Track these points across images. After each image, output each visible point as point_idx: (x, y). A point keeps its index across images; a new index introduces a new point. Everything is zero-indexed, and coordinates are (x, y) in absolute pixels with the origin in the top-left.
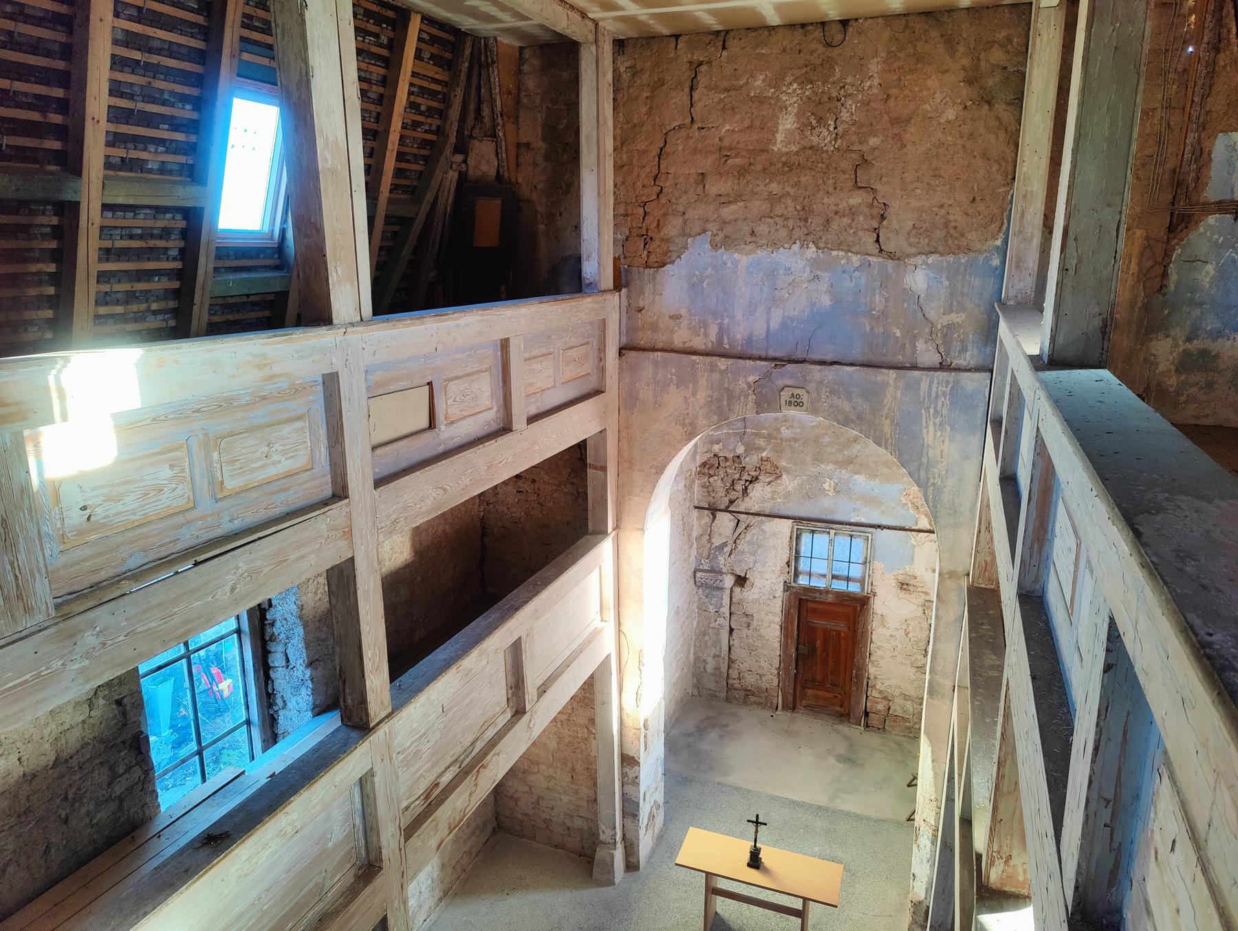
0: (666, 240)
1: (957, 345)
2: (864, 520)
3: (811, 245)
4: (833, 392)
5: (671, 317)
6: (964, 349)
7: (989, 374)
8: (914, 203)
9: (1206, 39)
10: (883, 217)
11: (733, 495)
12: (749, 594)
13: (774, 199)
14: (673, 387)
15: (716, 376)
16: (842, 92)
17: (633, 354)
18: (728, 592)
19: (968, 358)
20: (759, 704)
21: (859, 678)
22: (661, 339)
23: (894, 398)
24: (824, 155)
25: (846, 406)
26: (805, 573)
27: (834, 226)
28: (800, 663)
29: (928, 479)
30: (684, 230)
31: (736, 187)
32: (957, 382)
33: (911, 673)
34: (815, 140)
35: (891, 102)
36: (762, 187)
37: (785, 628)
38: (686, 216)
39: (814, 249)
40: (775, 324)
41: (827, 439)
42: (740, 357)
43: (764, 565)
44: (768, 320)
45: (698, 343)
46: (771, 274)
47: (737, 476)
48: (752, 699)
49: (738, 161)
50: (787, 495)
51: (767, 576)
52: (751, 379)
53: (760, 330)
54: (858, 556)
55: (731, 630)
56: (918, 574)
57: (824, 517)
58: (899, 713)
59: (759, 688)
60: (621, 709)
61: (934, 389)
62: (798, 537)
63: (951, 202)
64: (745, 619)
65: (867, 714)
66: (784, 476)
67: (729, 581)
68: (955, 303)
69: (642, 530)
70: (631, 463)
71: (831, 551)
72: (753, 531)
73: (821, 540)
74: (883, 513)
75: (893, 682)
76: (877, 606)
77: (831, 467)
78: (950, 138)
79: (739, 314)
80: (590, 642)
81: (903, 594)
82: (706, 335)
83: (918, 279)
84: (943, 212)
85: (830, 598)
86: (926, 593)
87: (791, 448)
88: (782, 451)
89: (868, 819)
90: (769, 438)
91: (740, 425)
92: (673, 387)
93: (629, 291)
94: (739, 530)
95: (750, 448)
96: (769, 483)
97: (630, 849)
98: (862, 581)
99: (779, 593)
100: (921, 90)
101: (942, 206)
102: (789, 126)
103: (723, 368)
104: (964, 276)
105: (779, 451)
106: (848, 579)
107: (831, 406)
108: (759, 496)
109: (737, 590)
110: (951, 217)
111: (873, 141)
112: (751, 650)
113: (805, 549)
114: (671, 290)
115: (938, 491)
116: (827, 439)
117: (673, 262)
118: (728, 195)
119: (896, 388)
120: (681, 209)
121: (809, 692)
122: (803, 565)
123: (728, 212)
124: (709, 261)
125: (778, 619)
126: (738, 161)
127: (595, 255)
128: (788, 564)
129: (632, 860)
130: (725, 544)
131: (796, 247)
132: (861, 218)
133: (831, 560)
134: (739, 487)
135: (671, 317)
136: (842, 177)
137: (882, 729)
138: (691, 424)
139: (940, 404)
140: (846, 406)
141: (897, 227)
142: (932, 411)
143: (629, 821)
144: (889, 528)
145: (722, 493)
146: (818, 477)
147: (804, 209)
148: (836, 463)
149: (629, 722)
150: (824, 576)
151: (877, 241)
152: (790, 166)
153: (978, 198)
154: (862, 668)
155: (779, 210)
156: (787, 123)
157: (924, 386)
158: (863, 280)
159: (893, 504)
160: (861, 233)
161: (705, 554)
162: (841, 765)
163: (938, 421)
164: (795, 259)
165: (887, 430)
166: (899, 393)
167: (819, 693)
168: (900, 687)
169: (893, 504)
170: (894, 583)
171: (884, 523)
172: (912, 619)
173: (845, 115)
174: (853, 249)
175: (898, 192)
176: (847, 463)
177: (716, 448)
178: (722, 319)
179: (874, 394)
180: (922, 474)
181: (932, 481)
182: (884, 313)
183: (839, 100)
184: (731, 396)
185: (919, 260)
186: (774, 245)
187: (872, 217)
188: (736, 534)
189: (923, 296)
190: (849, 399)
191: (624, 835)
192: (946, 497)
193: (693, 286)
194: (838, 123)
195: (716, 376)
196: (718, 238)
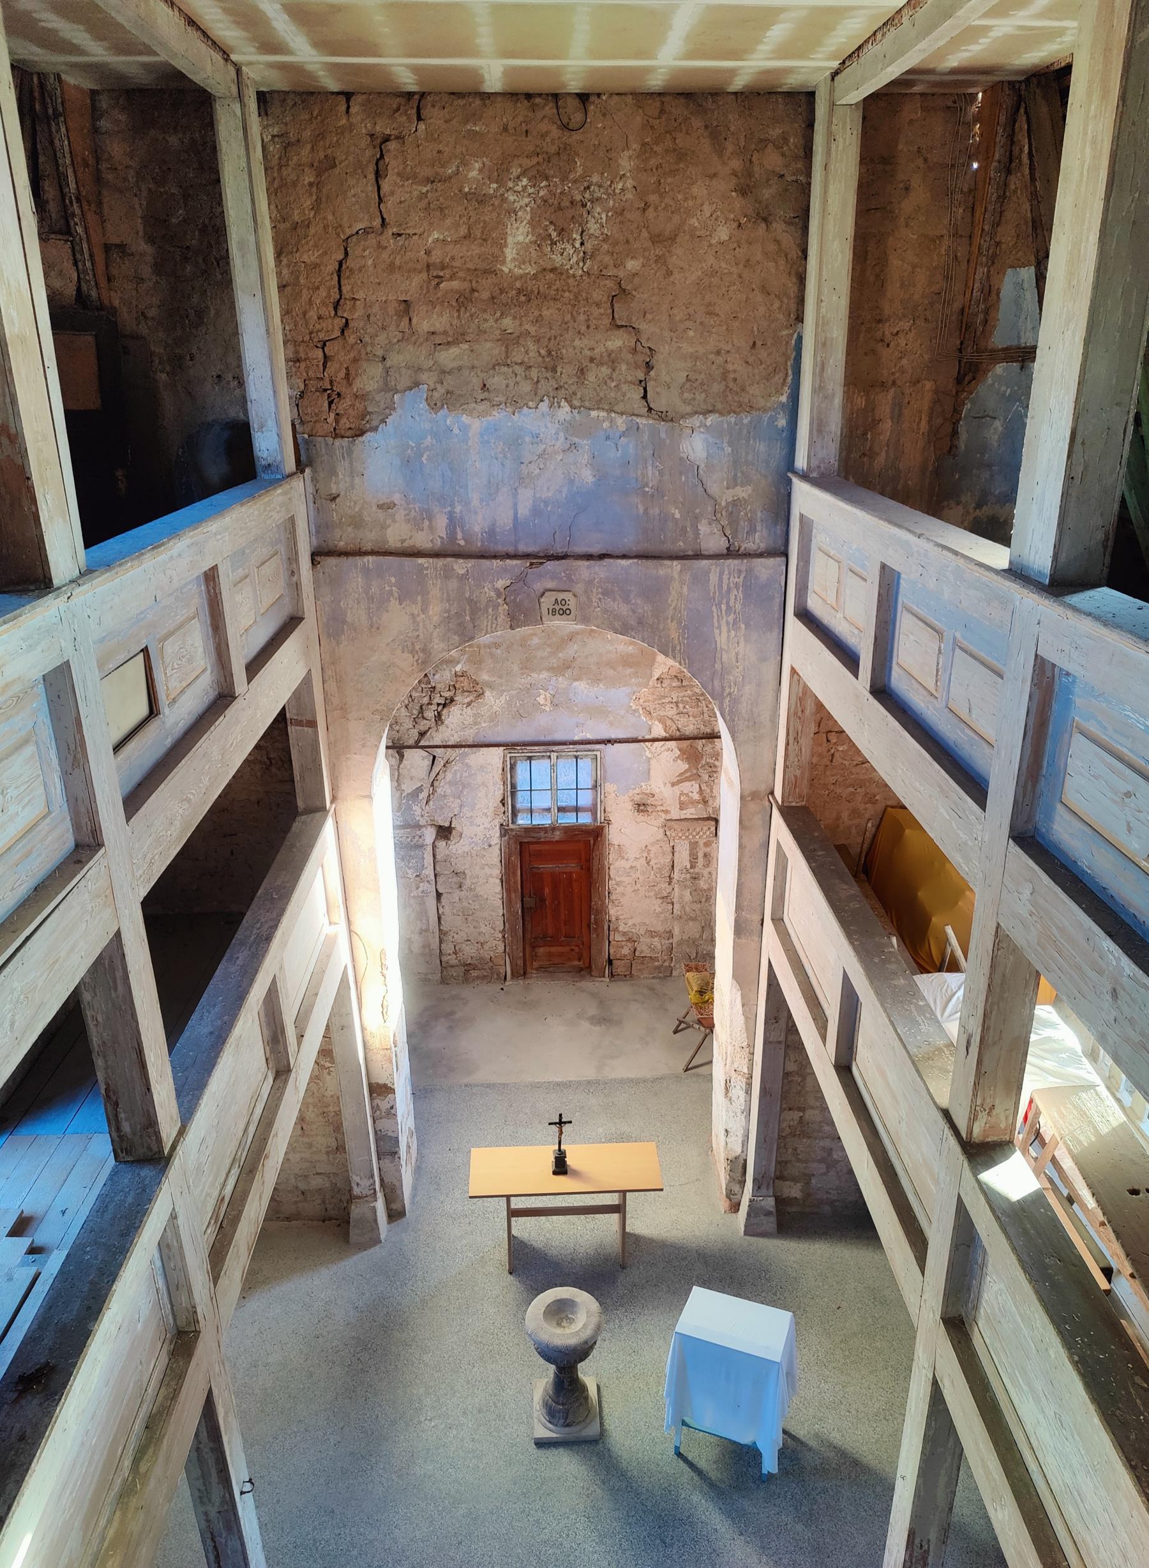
0: (361, 397)
1: (744, 525)
2: (589, 736)
3: (563, 403)
4: (606, 593)
5: (380, 507)
6: (752, 530)
7: (784, 559)
8: (687, 348)
9: (997, 156)
10: (649, 367)
11: (423, 725)
12: (456, 847)
13: (509, 341)
14: (394, 604)
15: (453, 584)
16: (587, 195)
17: (332, 561)
18: (430, 849)
19: (757, 541)
20: (484, 977)
21: (599, 923)
22: (369, 538)
23: (680, 595)
24: (571, 281)
25: (624, 610)
26: (524, 810)
27: (591, 377)
28: (527, 919)
29: (723, 688)
30: (386, 383)
31: (455, 322)
32: (750, 571)
33: (656, 905)
34: (558, 260)
35: (650, 213)
36: (491, 322)
37: (506, 881)
38: (388, 363)
39: (568, 409)
40: (524, 510)
42: (482, 556)
44: (515, 505)
45: (422, 540)
46: (515, 442)
47: (426, 700)
48: (474, 973)
49: (455, 284)
50: (494, 718)
51: (478, 821)
52: (501, 584)
53: (505, 519)
54: (586, 781)
55: (439, 895)
56: (656, 791)
57: (542, 738)
58: (647, 953)
59: (482, 959)
60: (363, 1029)
61: (725, 581)
63: (729, 347)
64: (455, 879)
65: (610, 962)
66: (487, 693)
67: (430, 835)
68: (739, 475)
69: (370, 797)
70: (344, 709)
71: (554, 780)
72: (455, 767)
73: (541, 767)
74: (611, 724)
75: (637, 920)
76: (614, 835)
77: (544, 675)
78: (724, 265)
79: (475, 499)
80: (329, 956)
81: (640, 817)
82: (431, 527)
83: (696, 445)
84: (719, 360)
85: (557, 836)
86: (667, 812)
87: (492, 655)
88: (481, 662)
89: (645, 1081)
92: (394, 604)
93: (314, 471)
94: (436, 769)
96: (469, 704)
97: (392, 1193)
98: (593, 810)
99: (496, 839)
100: (686, 199)
101: (718, 353)
102: (521, 238)
103: (461, 572)
104: (748, 440)
106: (577, 809)
107: (605, 611)
108: (458, 722)
109: (442, 844)
110: (730, 367)
111: (632, 265)
112: (466, 915)
114: (376, 469)
115: (735, 701)
116: (535, 641)
117: (375, 429)
118: (445, 333)
119: (682, 583)
120: (380, 353)
121: (541, 951)
122: (522, 801)
123: (448, 357)
124: (427, 426)
125: (497, 872)
126: (455, 284)
127: (271, 423)
128: (503, 802)
129: (394, 1206)
130: (420, 789)
131: (544, 406)
132: (624, 367)
133: (554, 789)
134: (430, 714)
135: (380, 507)
136: (596, 312)
137: (629, 976)
138: (424, 650)
139: (732, 598)
140: (624, 610)
141: (668, 379)
142: (724, 607)
143: (387, 1162)
144: (620, 741)
145: (408, 724)
146: (530, 689)
147: (549, 353)
149: (375, 1043)
150: (548, 810)
151: (645, 397)
152: (525, 296)
153: (759, 343)
154: (602, 911)
155: (517, 355)
156: (518, 235)
157: (714, 578)
158: (631, 449)
159: (622, 712)
160: (625, 387)
162: (598, 1028)
163: (731, 618)
164: (544, 422)
165: (674, 635)
166: (685, 589)
167: (553, 949)
169: (622, 712)
171: (613, 736)
172: (653, 844)
173: (593, 227)
174: (615, 408)
175: (666, 334)
176: (564, 667)
178: (452, 505)
179: (655, 592)
180: (716, 683)
181: (727, 690)
182: (659, 491)
183: (584, 206)
184: (475, 608)
185: (696, 420)
186: (515, 403)
187: (637, 367)
188: (433, 774)
189: (702, 466)
190: (627, 601)
191: (382, 1180)
192: (744, 708)
193: (407, 462)
194: (585, 238)
195: (453, 584)
196: (436, 395)
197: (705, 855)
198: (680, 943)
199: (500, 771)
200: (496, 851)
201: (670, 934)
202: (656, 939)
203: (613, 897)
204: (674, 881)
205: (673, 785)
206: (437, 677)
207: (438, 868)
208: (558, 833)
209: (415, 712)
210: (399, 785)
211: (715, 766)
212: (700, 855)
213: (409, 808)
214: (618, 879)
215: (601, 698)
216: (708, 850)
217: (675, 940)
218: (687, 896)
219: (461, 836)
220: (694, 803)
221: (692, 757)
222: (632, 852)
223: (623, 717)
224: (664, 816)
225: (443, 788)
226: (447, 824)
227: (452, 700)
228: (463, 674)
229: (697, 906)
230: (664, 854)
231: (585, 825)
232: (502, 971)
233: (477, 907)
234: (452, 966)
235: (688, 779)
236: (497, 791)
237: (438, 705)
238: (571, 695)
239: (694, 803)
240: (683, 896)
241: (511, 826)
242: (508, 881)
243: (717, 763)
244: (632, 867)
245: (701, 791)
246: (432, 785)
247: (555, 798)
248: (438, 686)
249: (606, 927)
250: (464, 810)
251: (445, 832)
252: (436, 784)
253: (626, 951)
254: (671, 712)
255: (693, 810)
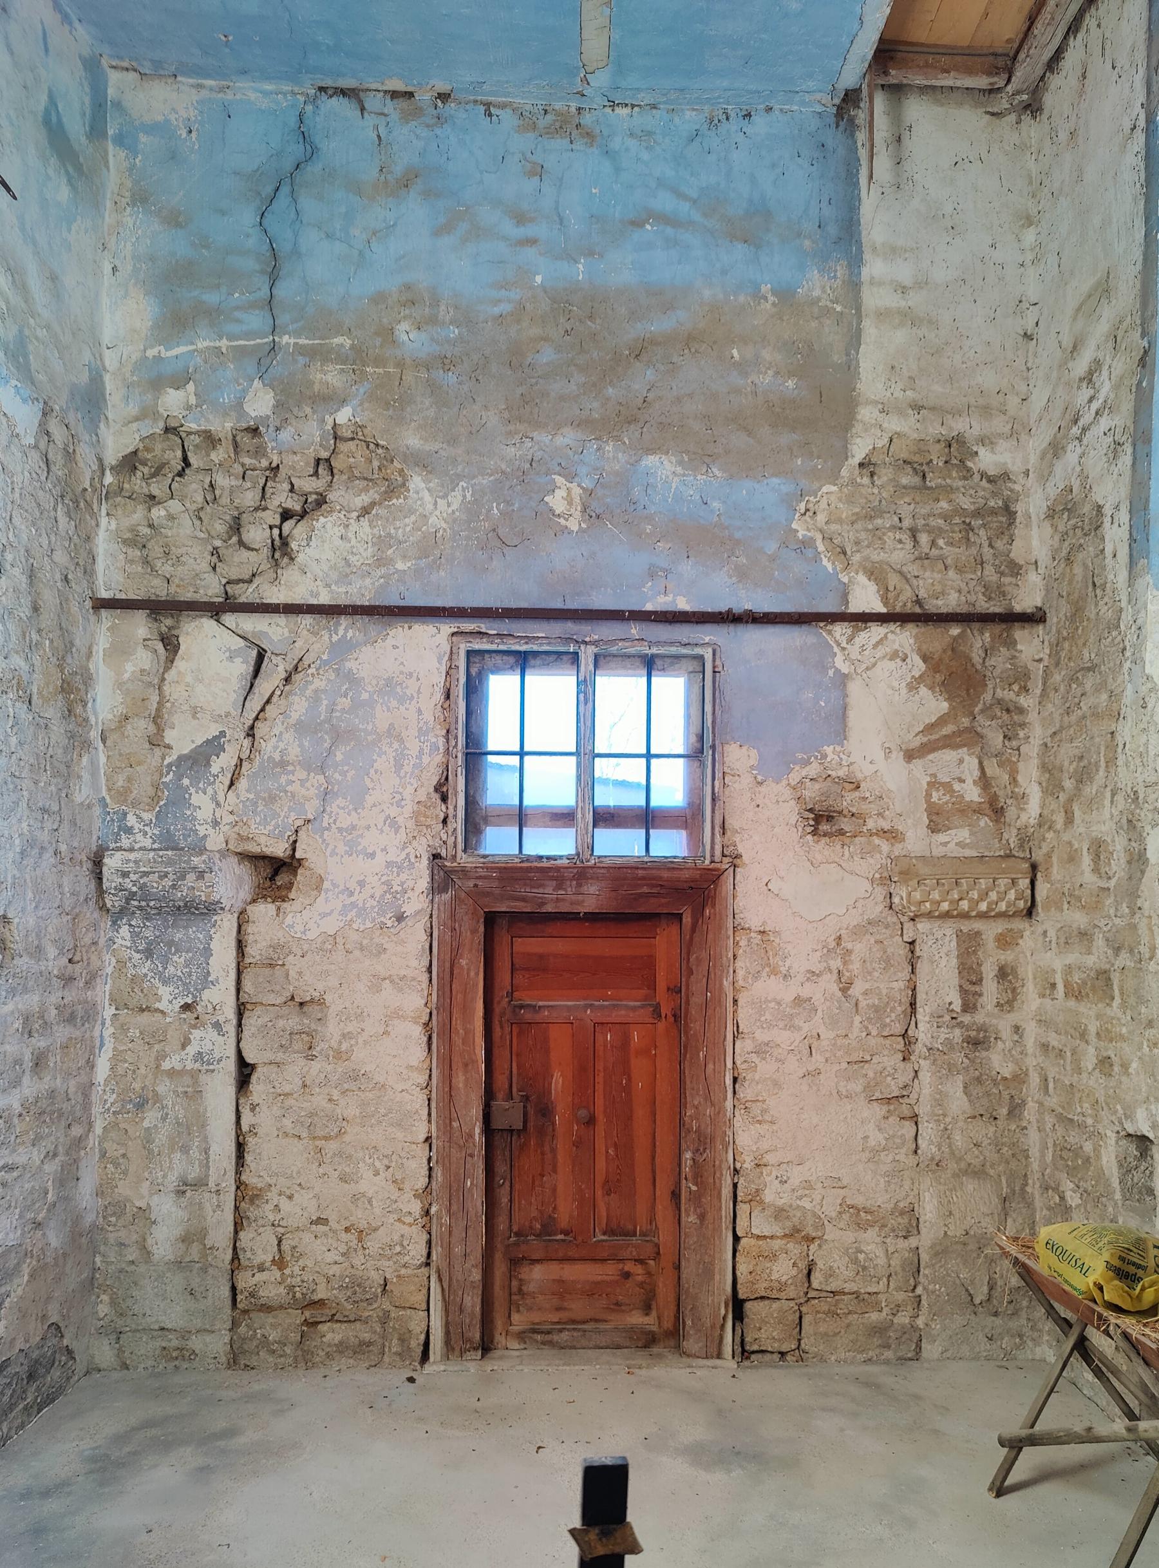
11: (240, 563)
12: (306, 918)
18: (227, 924)
20: (361, 1348)
33: (870, 1123)
37: (440, 1031)
41: (547, 356)
43: (358, 804)
47: (250, 498)
48: (332, 1334)
50: (429, 547)
51: (371, 840)
54: (672, 734)
55: (245, 1072)
56: (863, 770)
57: (558, 604)
58: (844, 1277)
59: (356, 1284)
62: (474, 690)
64: (293, 1022)
65: (738, 1307)
66: (416, 482)
67: (230, 884)
72: (317, 682)
74: (742, 574)
77: (568, 437)
81: (822, 849)
85: (591, 897)
86: (892, 835)
90: (357, 359)
91: (256, 320)
94: (265, 686)
95: (293, 398)
96: (365, 511)
98: (686, 819)
99: (417, 902)
105: (392, 401)
106: (648, 818)
108: (332, 555)
109: (263, 911)
113: (499, 732)
121: (537, 1275)
122: (499, 789)
130: (214, 746)
133: (585, 753)
134: (257, 534)
145: (196, 560)
146: (529, 477)
148: (583, 423)
150: (563, 818)
159: (771, 547)
161: (143, 788)
162: (718, 1477)
168: (837, 1183)
169: (771, 547)
170: (790, 812)
172: (858, 931)
177: (173, 401)
188: (255, 704)
197: (1003, 973)
198: (941, 1251)
199: (439, 696)
200: (415, 937)
201: (912, 1225)
202: (872, 1234)
203: (746, 1092)
204: (919, 1048)
205: (910, 755)
206: (285, 435)
207: (247, 985)
208: (592, 888)
209: (220, 528)
210: (160, 730)
211: (1021, 711)
212: (989, 971)
213: (180, 800)
214: (762, 1036)
215: (716, 505)
216: (1007, 957)
217: (926, 1239)
218: (958, 1102)
219: (318, 888)
220: (966, 811)
221: (957, 679)
222: (801, 953)
223: (773, 559)
224: (885, 847)
225: (278, 739)
226: (279, 850)
227: (321, 501)
228: (358, 434)
229: (984, 1131)
230: (887, 962)
231: (667, 864)
232: (417, 1326)
233: (352, 1111)
234: (267, 1308)
235: (948, 743)
236: (427, 754)
237: (286, 515)
238: (637, 492)
239: (966, 811)
240: (942, 1094)
241: (463, 859)
242: (447, 1031)
243: (1023, 701)
244: (798, 1001)
245: (984, 781)
246: (251, 733)
247: (586, 781)
248: (289, 459)
249: (726, 1191)
250: (334, 806)
251: (276, 873)
252: (261, 729)
253: (783, 1270)
254: (898, 554)
255: (963, 834)
